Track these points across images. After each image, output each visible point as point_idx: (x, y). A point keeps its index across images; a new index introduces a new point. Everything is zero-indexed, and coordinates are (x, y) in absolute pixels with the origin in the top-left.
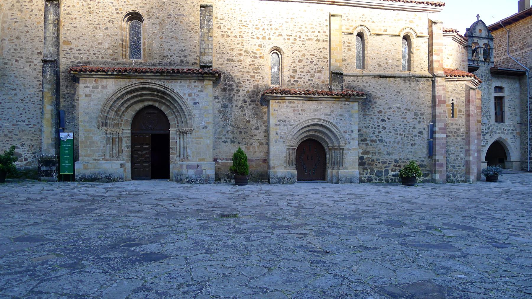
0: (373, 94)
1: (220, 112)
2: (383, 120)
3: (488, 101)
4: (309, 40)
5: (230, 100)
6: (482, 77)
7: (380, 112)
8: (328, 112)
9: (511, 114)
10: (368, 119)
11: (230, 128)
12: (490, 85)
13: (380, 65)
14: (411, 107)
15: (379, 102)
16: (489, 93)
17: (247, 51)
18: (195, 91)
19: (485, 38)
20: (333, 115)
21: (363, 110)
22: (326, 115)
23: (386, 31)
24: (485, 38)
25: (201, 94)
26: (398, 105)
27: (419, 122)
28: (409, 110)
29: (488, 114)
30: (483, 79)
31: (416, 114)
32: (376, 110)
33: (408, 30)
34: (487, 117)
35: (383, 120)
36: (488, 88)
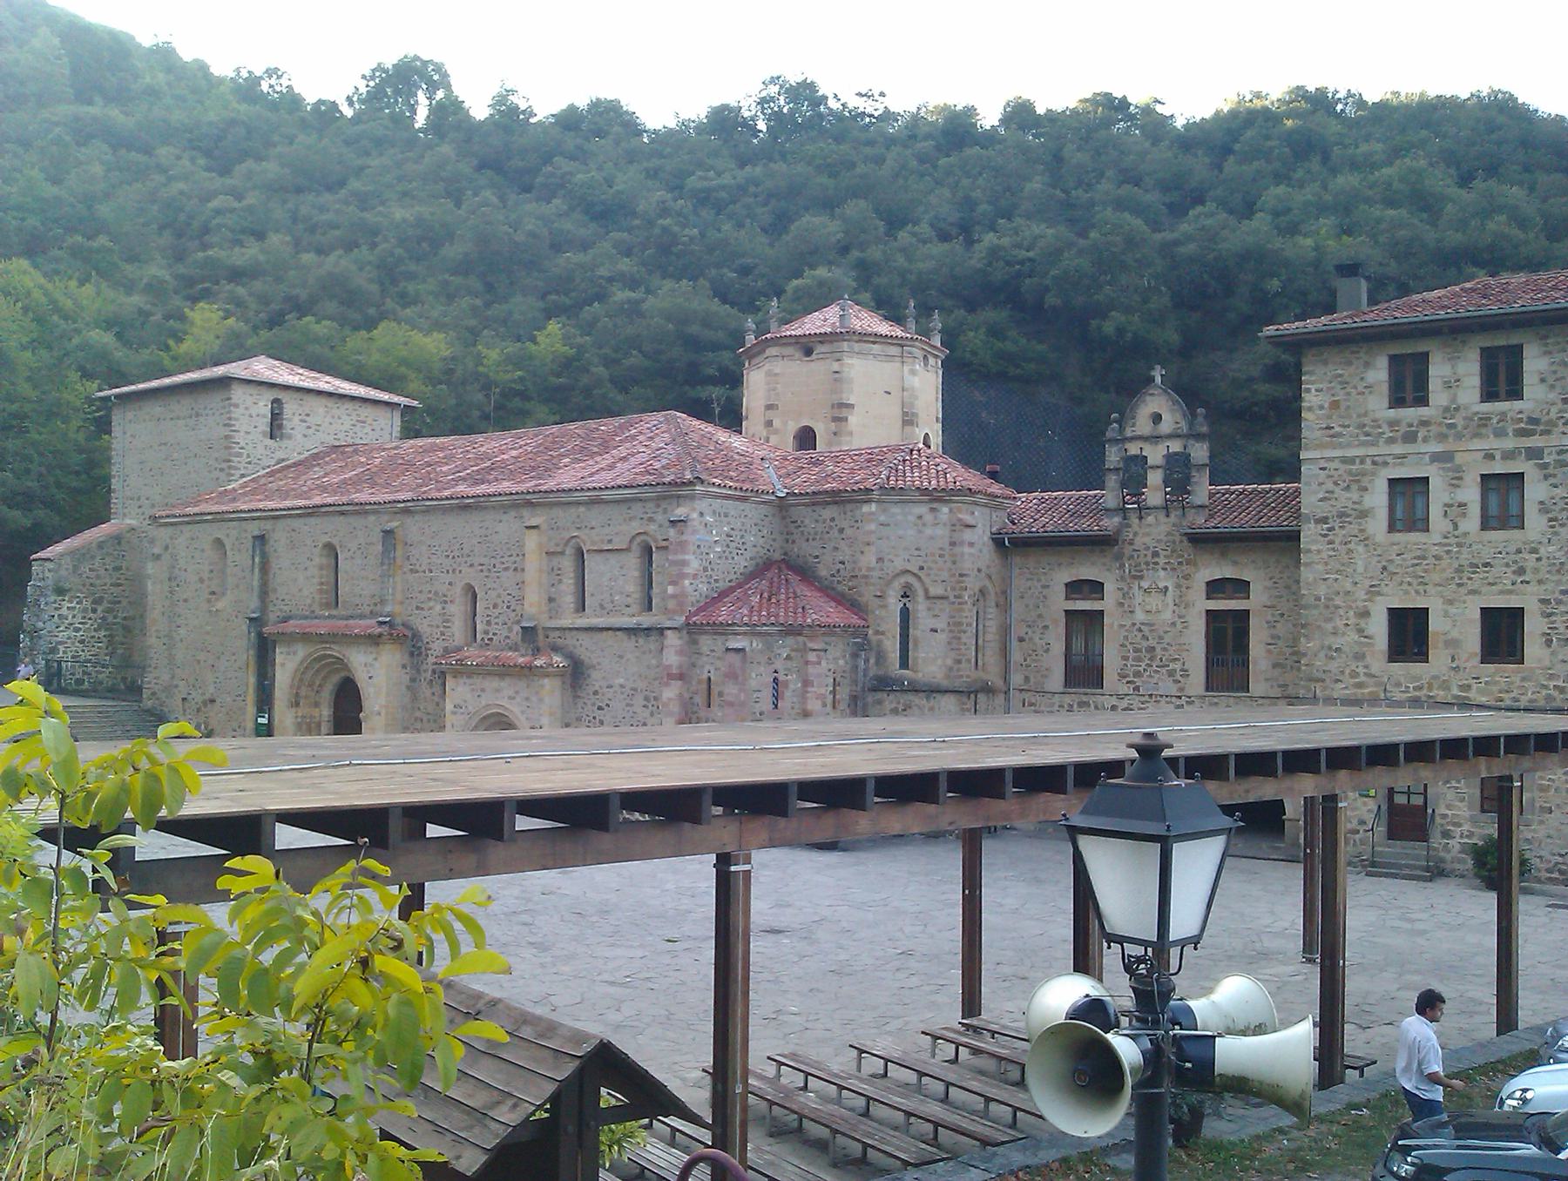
0: (587, 661)
1: (408, 688)
2: (600, 708)
3: (1179, 626)
4: (506, 569)
5: (418, 671)
6: (1156, 554)
7: (596, 693)
8: (511, 693)
9: (1275, 666)
10: (580, 705)
11: (418, 714)
12: (1187, 577)
13: (602, 606)
14: (641, 685)
15: (595, 675)
16: (1181, 603)
17: (436, 593)
18: (370, 658)
19: (1170, 436)
20: (518, 699)
21: (573, 687)
22: (510, 698)
23: (610, 541)
24: (1170, 436)
25: (377, 664)
26: (622, 681)
27: (652, 714)
28: (635, 689)
29: (1178, 666)
30: (1162, 561)
31: (647, 699)
32: (591, 690)
33: (638, 539)
34: (1171, 673)
35: (600, 708)
36: (1178, 586)
